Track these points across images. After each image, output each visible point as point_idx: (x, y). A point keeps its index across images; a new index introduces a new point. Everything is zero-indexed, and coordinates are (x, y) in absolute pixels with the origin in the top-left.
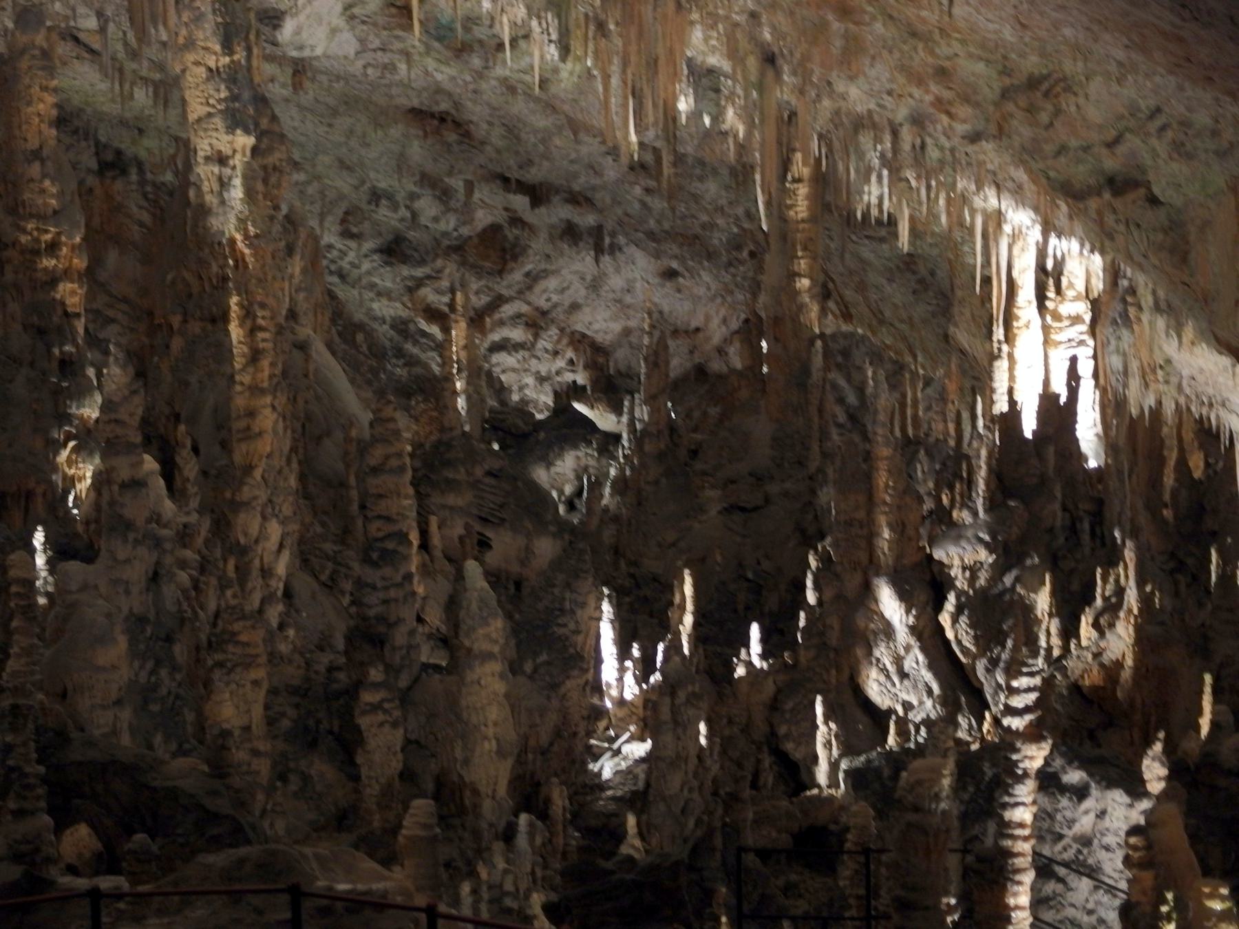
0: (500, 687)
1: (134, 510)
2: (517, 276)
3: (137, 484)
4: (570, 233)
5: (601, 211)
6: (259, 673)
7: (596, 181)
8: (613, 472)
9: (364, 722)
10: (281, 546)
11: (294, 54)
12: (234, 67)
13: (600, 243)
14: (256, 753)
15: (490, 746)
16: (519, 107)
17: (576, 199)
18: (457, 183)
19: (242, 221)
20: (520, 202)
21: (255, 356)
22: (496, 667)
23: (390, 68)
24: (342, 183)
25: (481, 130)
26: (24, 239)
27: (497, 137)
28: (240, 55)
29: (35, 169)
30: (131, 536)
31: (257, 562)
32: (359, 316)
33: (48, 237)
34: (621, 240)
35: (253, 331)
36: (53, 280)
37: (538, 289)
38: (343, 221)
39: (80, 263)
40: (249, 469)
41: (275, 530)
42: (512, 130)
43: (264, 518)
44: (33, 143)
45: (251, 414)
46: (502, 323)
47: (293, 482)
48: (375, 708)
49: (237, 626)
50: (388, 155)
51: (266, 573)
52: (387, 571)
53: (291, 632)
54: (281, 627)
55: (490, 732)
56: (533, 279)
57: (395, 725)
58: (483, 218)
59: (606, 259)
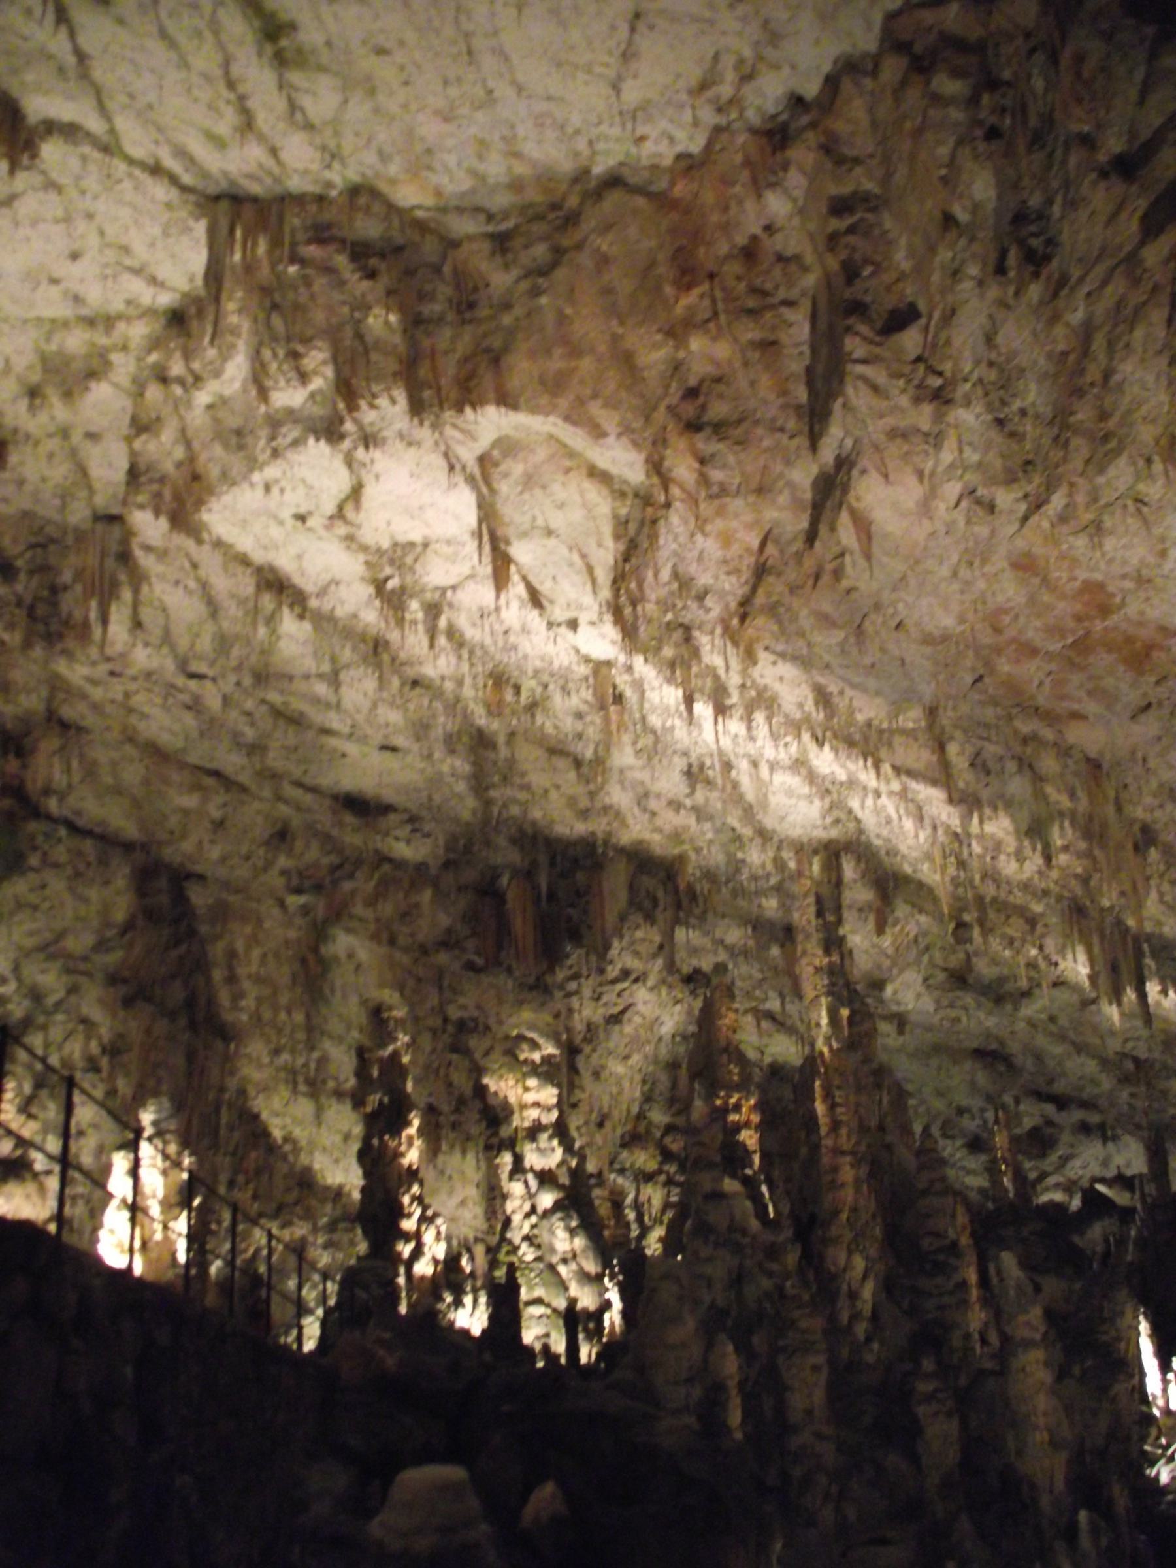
0: (1044, 1376)
1: (716, 1216)
2: (1053, 1158)
3: (718, 1196)
4: (1085, 1129)
5: (1101, 1112)
6: (820, 1359)
7: (1096, 1091)
8: (1133, 1233)
9: (921, 1410)
10: (865, 1277)
11: (894, 1008)
12: (831, 965)
13: (1104, 1133)
14: (819, 1436)
15: (1041, 1437)
16: (1041, 1041)
17: (1086, 1105)
18: (1008, 1099)
19: (827, 1040)
20: (1050, 1109)
21: (835, 1125)
22: (1038, 1354)
23: (958, 1020)
24: (938, 1104)
25: (1019, 1060)
26: (718, 1102)
27: (1029, 1064)
28: (835, 958)
29: (725, 1058)
30: (712, 1238)
31: (845, 1287)
32: (957, 1186)
33: (733, 1100)
34: (1119, 1131)
35: (832, 1107)
36: (737, 1128)
37: (1069, 1165)
38: (942, 1128)
39: (755, 1118)
40: (836, 1213)
41: (859, 1263)
42: (1039, 1057)
43: (850, 1252)
44: (723, 1043)
45: (835, 1169)
46: (1047, 1189)
47: (878, 1232)
48: (930, 1398)
49: (797, 1314)
50: (962, 1083)
51: (853, 1296)
52: (939, 1280)
53: (876, 1346)
54: (868, 1340)
55: (1041, 1421)
56: (1065, 1160)
57: (949, 1415)
58: (1028, 1123)
59: (1110, 1145)
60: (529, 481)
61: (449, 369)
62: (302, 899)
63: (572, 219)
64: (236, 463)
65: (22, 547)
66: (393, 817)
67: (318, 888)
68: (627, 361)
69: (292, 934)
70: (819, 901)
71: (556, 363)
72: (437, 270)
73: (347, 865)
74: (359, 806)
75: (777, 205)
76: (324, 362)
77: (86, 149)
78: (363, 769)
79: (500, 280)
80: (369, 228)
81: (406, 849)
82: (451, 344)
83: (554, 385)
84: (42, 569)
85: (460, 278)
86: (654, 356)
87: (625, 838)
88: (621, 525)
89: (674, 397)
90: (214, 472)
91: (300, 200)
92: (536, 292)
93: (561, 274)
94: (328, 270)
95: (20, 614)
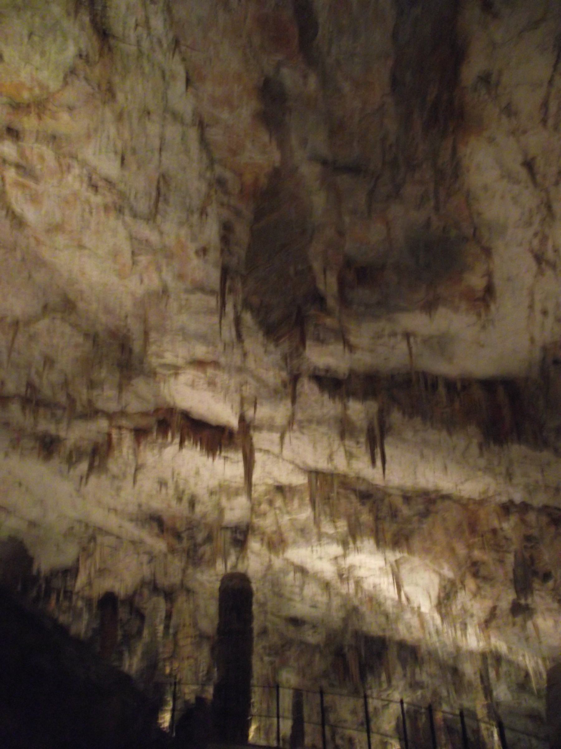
60: (412, 570)
61: (389, 536)
62: (270, 659)
63: (432, 502)
64: (301, 540)
65: (184, 529)
66: (306, 626)
67: (277, 654)
68: (453, 550)
69: (265, 672)
70: (481, 677)
71: (428, 544)
72: (382, 500)
73: (287, 644)
74: (296, 622)
75: (505, 526)
76: (343, 526)
77: (271, 457)
78: (300, 609)
79: (405, 511)
80: (363, 487)
81: (312, 638)
82: (390, 528)
83: (427, 551)
84: (192, 537)
85: (391, 506)
86: (461, 551)
87: (397, 638)
88: (443, 588)
89: (469, 564)
90: (290, 540)
91: (338, 475)
92: (420, 522)
93: (430, 519)
94: (347, 497)
95: (184, 555)
